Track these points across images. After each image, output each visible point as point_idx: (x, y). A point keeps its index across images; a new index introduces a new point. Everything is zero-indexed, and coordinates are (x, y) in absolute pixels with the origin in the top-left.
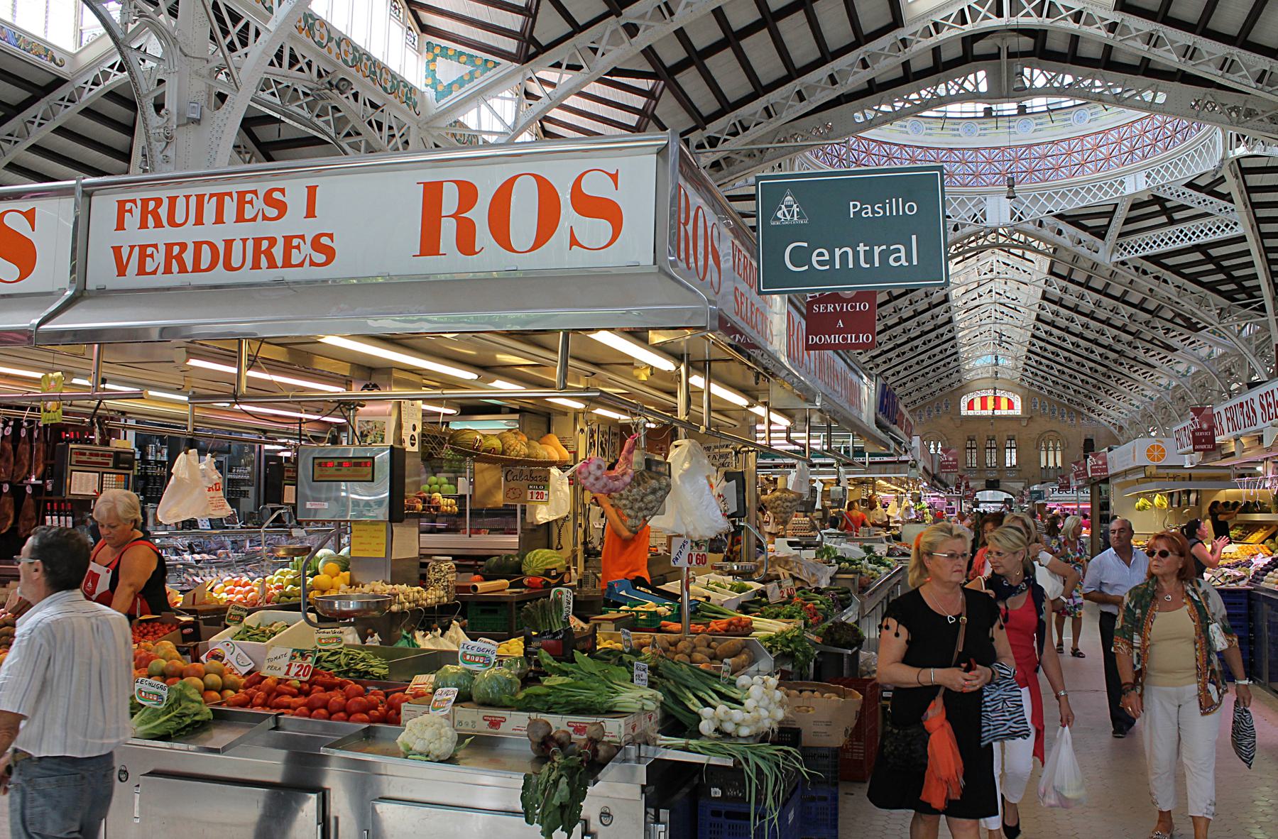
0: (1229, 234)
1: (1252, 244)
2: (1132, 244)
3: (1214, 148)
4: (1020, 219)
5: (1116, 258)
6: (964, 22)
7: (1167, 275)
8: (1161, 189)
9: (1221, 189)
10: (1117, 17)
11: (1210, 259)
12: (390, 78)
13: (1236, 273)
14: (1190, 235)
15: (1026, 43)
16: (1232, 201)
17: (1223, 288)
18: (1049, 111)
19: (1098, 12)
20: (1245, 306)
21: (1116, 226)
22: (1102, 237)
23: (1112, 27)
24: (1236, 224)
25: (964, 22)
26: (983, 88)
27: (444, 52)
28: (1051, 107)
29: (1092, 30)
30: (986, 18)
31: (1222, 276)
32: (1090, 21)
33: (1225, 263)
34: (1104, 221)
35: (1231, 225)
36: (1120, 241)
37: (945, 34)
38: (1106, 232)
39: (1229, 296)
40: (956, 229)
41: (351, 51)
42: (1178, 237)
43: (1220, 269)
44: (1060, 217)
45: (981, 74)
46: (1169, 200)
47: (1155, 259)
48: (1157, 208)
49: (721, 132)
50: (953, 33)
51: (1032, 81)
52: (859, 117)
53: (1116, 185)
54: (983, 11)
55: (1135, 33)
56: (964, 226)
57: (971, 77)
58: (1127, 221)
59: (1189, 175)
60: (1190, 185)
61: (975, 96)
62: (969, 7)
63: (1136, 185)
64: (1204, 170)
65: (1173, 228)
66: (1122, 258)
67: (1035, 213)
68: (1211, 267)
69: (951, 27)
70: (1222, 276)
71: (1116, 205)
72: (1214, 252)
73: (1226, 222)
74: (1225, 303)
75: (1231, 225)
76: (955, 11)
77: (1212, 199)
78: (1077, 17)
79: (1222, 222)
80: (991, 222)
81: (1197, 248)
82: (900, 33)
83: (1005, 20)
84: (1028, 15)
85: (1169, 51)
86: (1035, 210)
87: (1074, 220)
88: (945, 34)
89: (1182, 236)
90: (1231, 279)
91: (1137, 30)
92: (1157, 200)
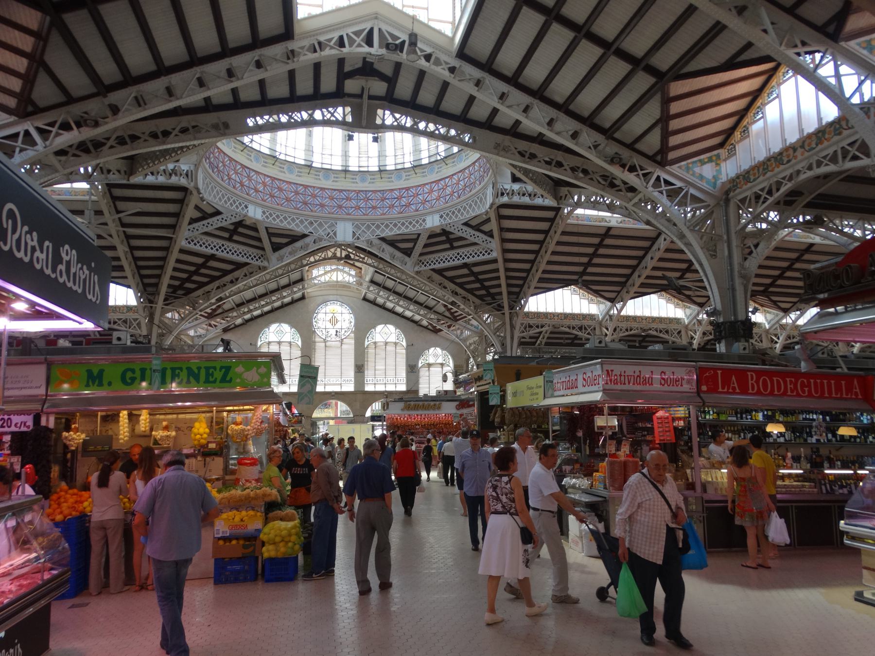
0: (487, 257)
1: (500, 265)
2: (428, 260)
3: (485, 198)
4: (358, 238)
5: (416, 269)
7: (447, 283)
8: (449, 226)
9: (486, 228)
10: (457, 63)
11: (473, 274)
13: (487, 284)
14: (463, 256)
16: (492, 236)
18: (380, 171)
19: (443, 57)
20: (490, 304)
21: (419, 248)
22: (409, 255)
23: (452, 70)
24: (491, 251)
26: (349, 119)
28: (382, 168)
29: (439, 69)
30: (359, 45)
31: (478, 285)
32: (438, 62)
33: (481, 277)
34: (410, 245)
36: (423, 258)
37: (327, 52)
38: (412, 252)
39: (480, 297)
42: (456, 257)
43: (478, 281)
44: (383, 239)
45: (348, 109)
46: (453, 233)
47: (439, 272)
48: (444, 238)
50: (334, 52)
51: (383, 120)
52: (250, 122)
53: (421, 221)
54: (358, 40)
55: (468, 77)
56: (321, 240)
58: (426, 246)
59: (466, 216)
60: (466, 224)
61: (342, 124)
63: (433, 222)
64: (479, 213)
65: (455, 252)
66: (420, 269)
67: (368, 235)
68: (472, 278)
69: (332, 48)
70: (478, 285)
71: (419, 235)
72: (476, 269)
73: (486, 249)
74: (478, 301)
76: (336, 35)
79: (483, 249)
80: (340, 238)
81: (465, 265)
86: (368, 233)
87: (392, 243)
88: (327, 52)
89: (458, 257)
90: (484, 287)
91: (470, 75)
92: (445, 232)
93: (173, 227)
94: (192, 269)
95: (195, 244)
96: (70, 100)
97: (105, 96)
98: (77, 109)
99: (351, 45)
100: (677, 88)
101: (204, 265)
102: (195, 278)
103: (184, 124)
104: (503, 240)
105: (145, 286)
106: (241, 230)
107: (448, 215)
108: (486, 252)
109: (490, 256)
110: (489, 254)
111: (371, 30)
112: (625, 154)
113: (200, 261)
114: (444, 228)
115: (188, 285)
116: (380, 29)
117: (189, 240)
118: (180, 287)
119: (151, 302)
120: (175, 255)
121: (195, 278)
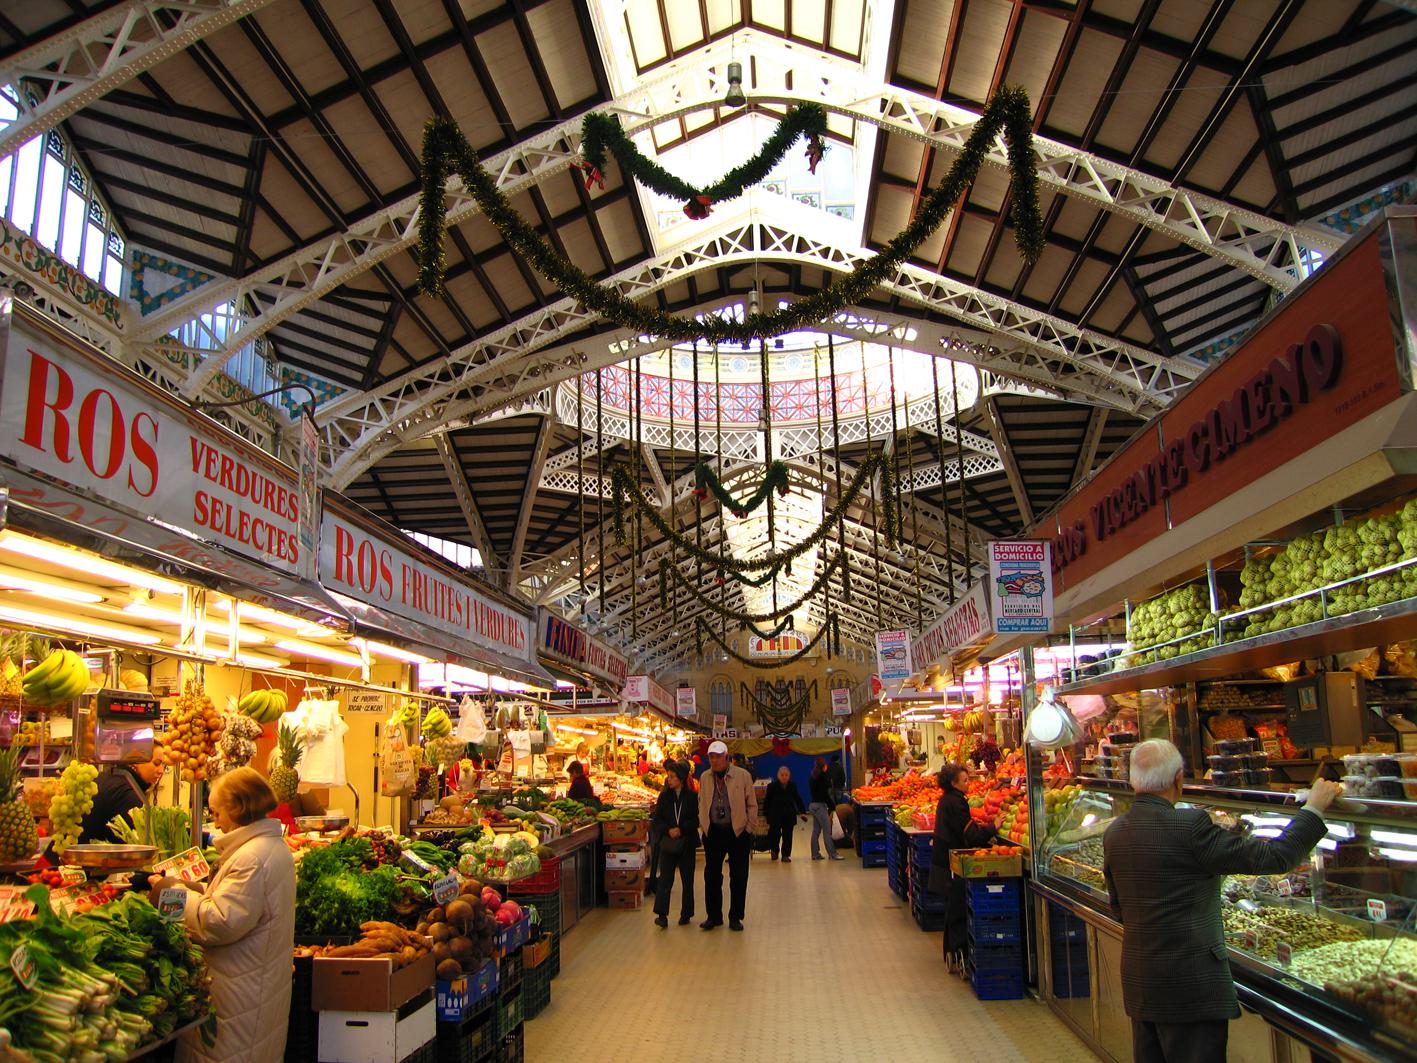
0: (990, 470)
1: (1013, 481)
4: (791, 455)
6: (717, 254)
9: (982, 426)
11: (975, 495)
12: (85, 286)
13: (1002, 509)
15: (781, 278)
16: (990, 438)
17: (990, 523)
24: (996, 460)
25: (717, 254)
27: (152, 263)
30: (737, 250)
31: (987, 512)
33: (991, 499)
35: (993, 461)
37: (697, 265)
40: (727, 464)
41: (35, 253)
43: (985, 505)
48: (922, 445)
49: (466, 359)
52: (613, 349)
56: (735, 461)
57: (729, 310)
62: (721, 240)
69: (702, 259)
70: (987, 512)
72: (980, 488)
75: (993, 461)
77: (972, 436)
78: (825, 253)
82: (651, 264)
83: (757, 253)
84: (778, 249)
85: (913, 289)
90: (996, 514)
93: (528, 463)
94: (555, 516)
95: (557, 484)
96: (414, 365)
97: (448, 356)
98: (419, 374)
99: (725, 252)
100: (1143, 271)
101: (570, 510)
102: (560, 528)
103: (533, 364)
104: (1013, 443)
105: (494, 543)
106: (617, 457)
107: (922, 409)
108: (988, 462)
109: (995, 469)
110: (993, 466)
111: (751, 228)
112: (1113, 345)
113: (564, 504)
114: (919, 427)
115: (550, 539)
116: (762, 227)
117: (549, 479)
118: (540, 542)
119: (503, 566)
120: (531, 499)
121: (560, 528)
